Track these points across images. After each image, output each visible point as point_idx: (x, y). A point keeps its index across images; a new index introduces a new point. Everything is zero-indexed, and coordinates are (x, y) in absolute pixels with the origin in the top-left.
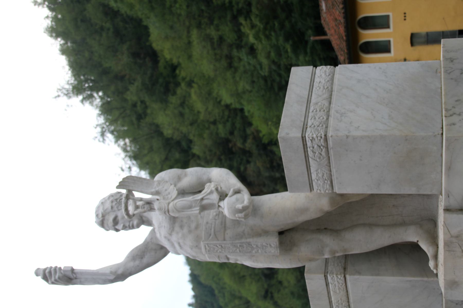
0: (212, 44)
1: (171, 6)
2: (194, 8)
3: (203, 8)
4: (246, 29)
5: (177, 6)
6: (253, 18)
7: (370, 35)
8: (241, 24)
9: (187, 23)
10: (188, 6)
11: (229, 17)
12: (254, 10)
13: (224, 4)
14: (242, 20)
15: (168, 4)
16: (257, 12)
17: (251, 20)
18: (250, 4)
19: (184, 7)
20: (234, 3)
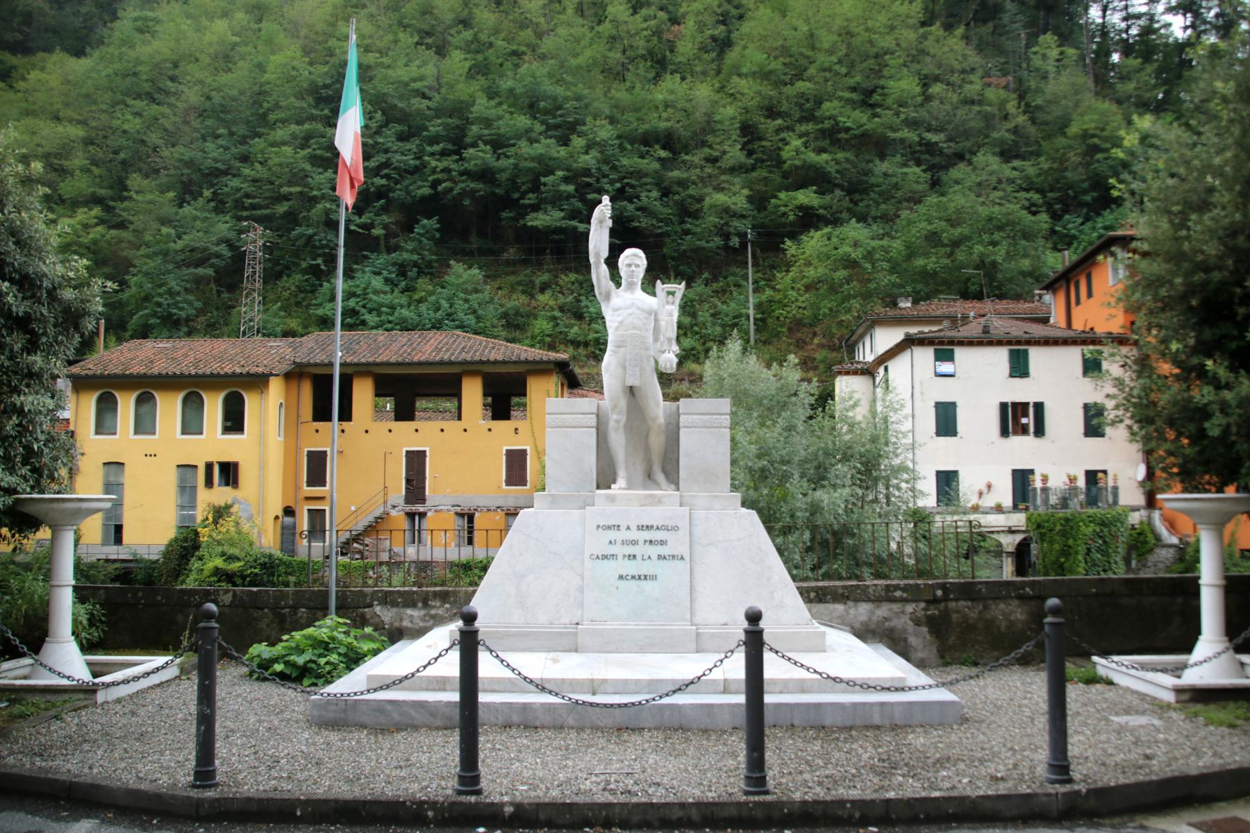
0: (58, 156)
1: (127, 106)
2: (123, 142)
3: (122, 155)
4: (82, 215)
5: (129, 117)
6: (99, 229)
7: (126, 404)
8: (90, 209)
9: (94, 124)
10: (125, 132)
11: (102, 192)
12: (113, 232)
13: (126, 189)
14: (97, 211)
15: (130, 102)
16: (108, 237)
17: (97, 225)
18: (122, 225)
19: (126, 127)
20: (126, 204)
